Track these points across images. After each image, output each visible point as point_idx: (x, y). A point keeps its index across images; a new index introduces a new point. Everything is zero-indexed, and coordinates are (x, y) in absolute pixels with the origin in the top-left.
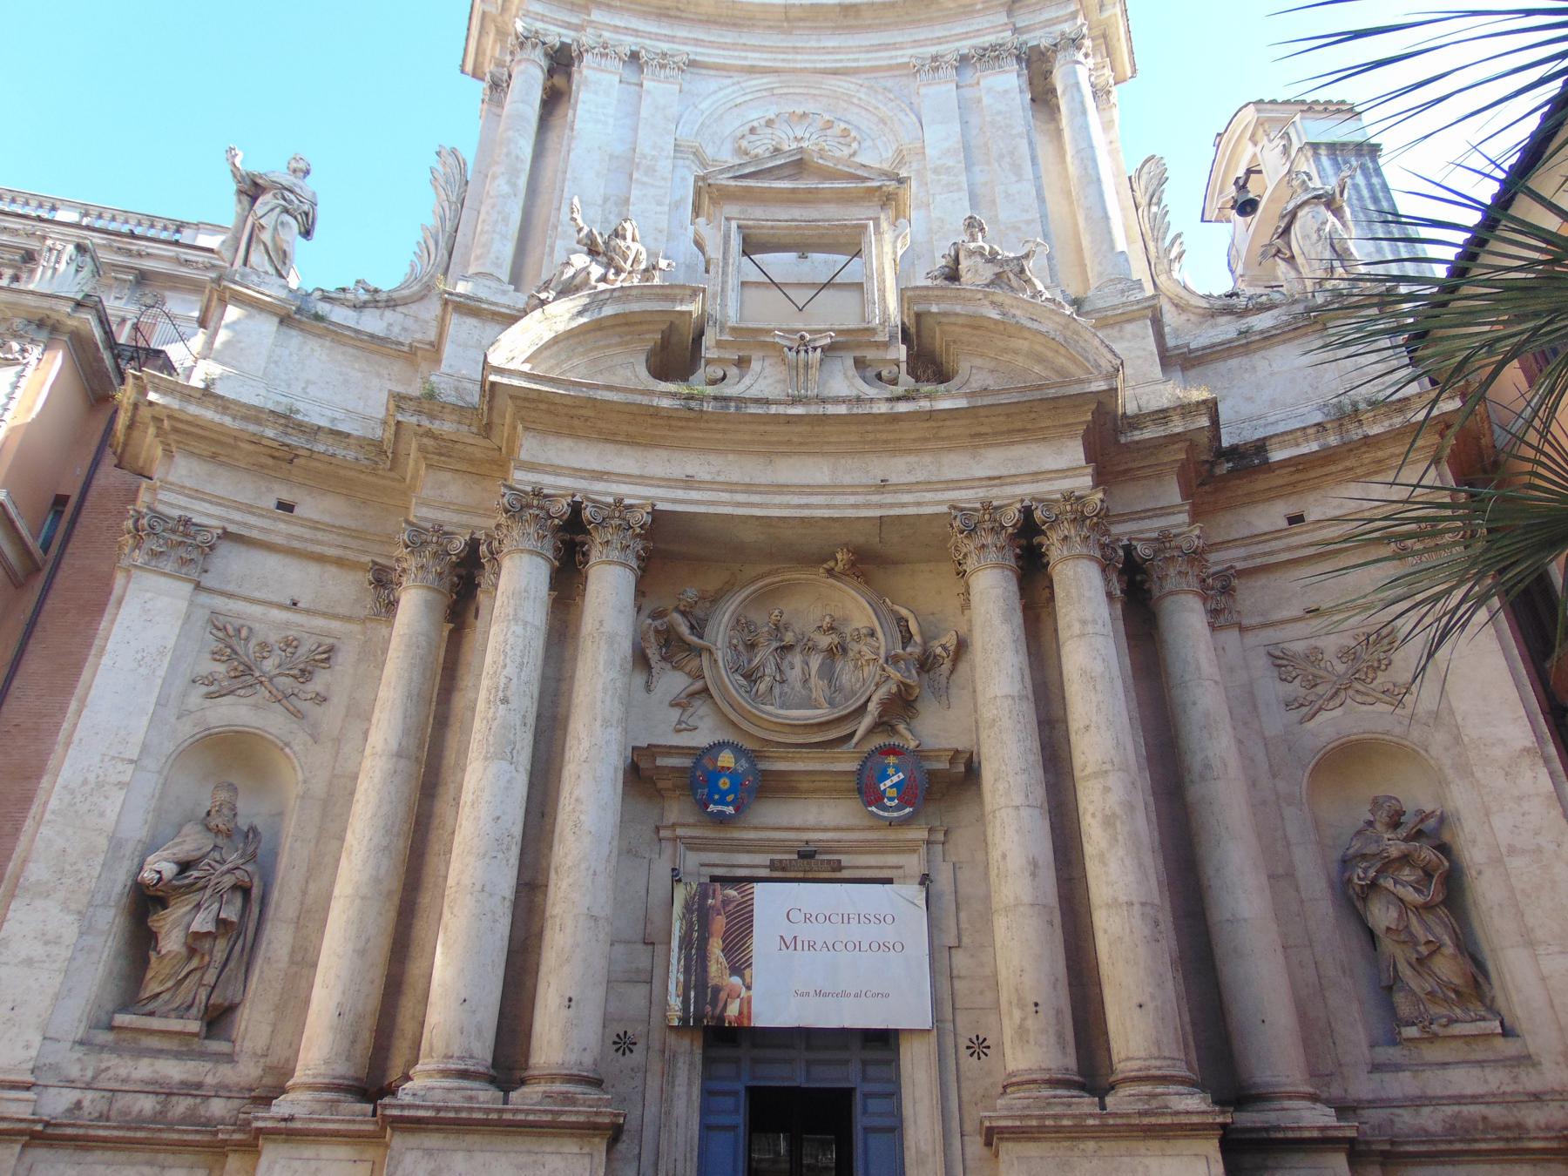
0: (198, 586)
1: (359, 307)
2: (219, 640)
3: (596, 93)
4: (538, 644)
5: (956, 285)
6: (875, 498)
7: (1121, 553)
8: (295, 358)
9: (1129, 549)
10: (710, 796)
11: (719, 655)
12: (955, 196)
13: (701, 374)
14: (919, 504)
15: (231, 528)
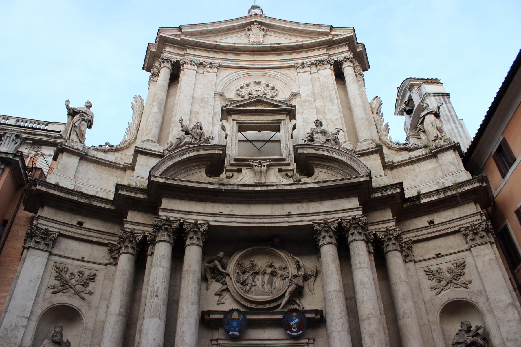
0: (51, 254)
1: (106, 152)
2: (57, 272)
3: (188, 77)
4: (168, 274)
5: (312, 143)
6: (286, 219)
7: (373, 236)
8: (84, 171)
9: (375, 235)
11: (232, 276)
12: (311, 110)
13: (223, 175)
14: (302, 221)
15: (62, 232)
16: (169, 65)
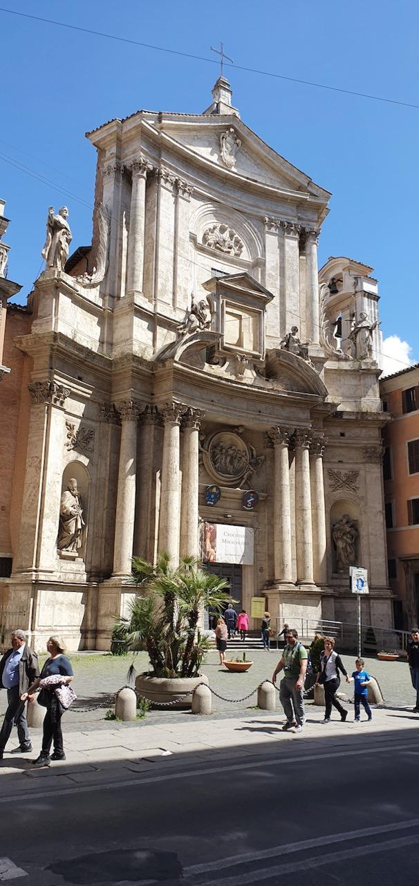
16: (145, 175)
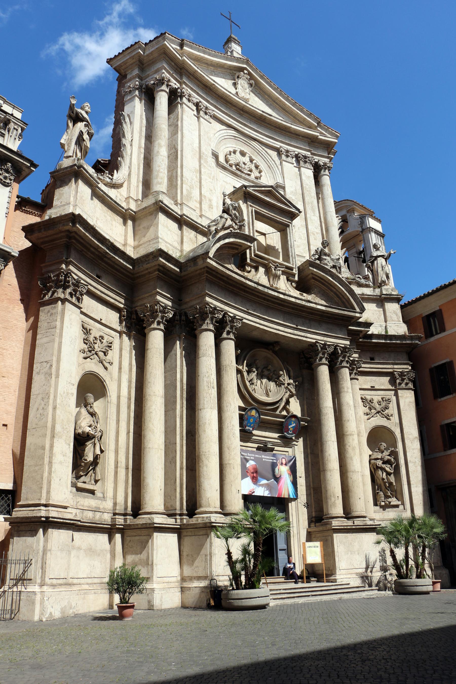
6: (296, 332)
10: (247, 423)
14: (306, 337)
